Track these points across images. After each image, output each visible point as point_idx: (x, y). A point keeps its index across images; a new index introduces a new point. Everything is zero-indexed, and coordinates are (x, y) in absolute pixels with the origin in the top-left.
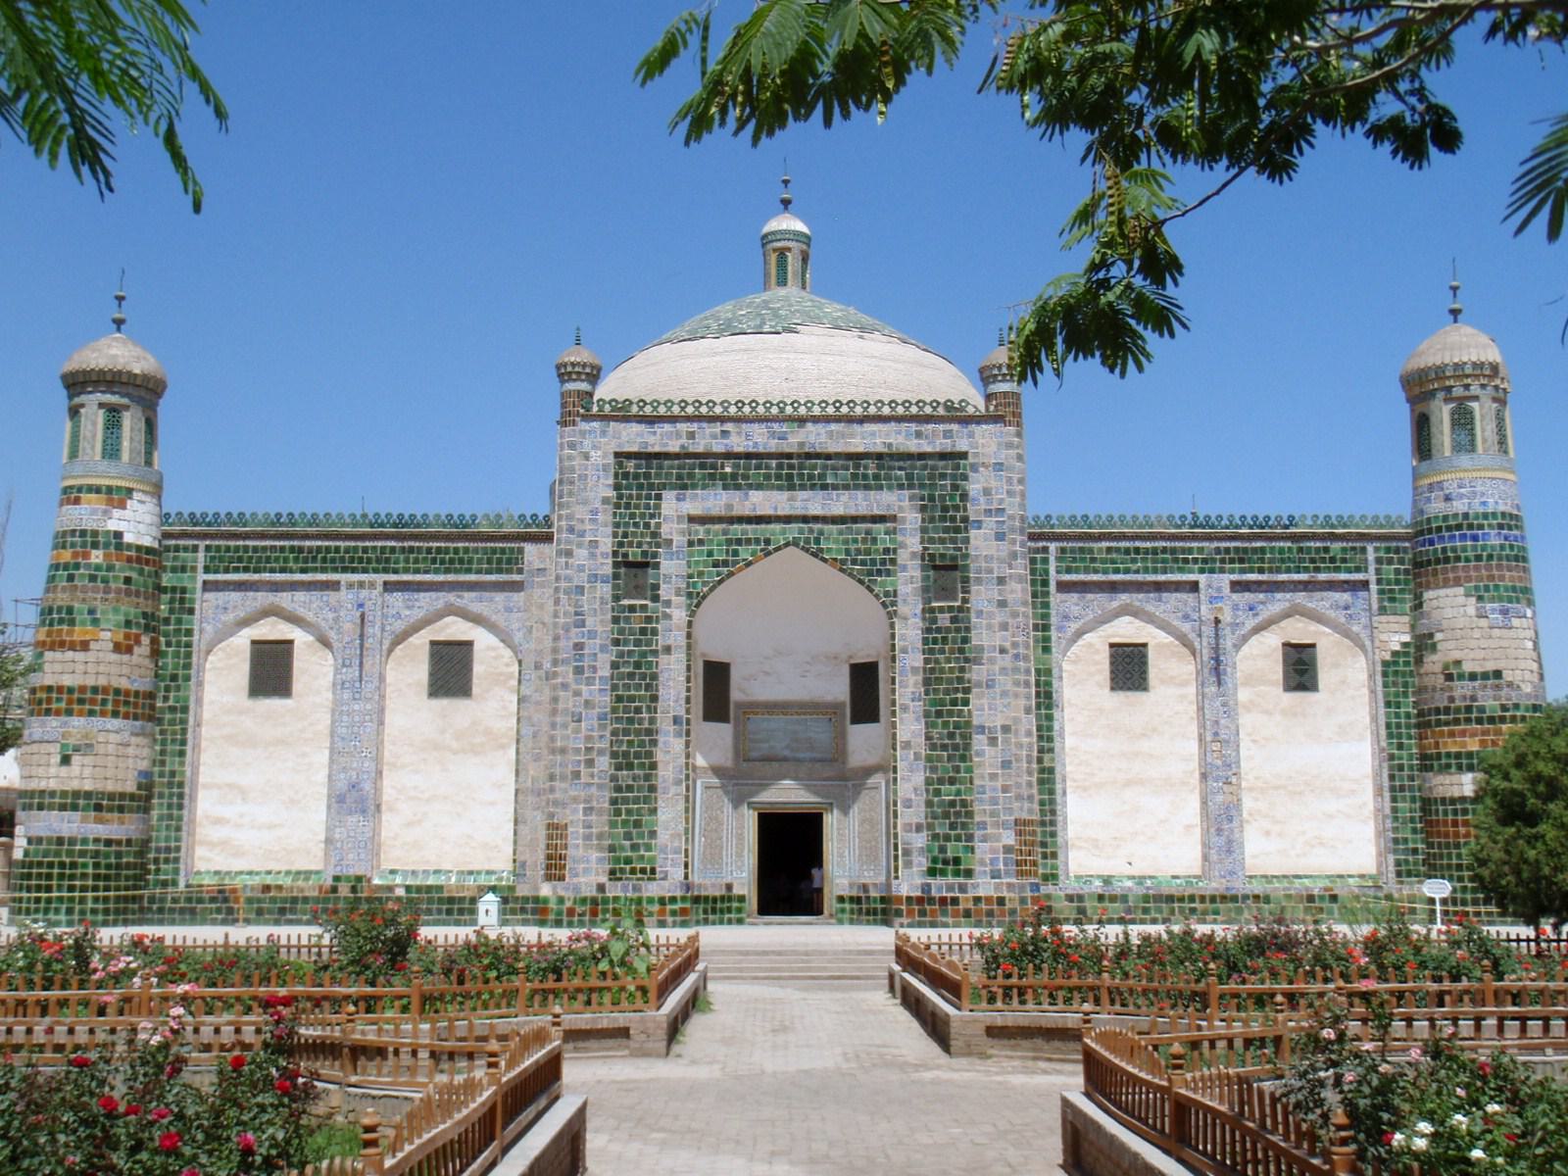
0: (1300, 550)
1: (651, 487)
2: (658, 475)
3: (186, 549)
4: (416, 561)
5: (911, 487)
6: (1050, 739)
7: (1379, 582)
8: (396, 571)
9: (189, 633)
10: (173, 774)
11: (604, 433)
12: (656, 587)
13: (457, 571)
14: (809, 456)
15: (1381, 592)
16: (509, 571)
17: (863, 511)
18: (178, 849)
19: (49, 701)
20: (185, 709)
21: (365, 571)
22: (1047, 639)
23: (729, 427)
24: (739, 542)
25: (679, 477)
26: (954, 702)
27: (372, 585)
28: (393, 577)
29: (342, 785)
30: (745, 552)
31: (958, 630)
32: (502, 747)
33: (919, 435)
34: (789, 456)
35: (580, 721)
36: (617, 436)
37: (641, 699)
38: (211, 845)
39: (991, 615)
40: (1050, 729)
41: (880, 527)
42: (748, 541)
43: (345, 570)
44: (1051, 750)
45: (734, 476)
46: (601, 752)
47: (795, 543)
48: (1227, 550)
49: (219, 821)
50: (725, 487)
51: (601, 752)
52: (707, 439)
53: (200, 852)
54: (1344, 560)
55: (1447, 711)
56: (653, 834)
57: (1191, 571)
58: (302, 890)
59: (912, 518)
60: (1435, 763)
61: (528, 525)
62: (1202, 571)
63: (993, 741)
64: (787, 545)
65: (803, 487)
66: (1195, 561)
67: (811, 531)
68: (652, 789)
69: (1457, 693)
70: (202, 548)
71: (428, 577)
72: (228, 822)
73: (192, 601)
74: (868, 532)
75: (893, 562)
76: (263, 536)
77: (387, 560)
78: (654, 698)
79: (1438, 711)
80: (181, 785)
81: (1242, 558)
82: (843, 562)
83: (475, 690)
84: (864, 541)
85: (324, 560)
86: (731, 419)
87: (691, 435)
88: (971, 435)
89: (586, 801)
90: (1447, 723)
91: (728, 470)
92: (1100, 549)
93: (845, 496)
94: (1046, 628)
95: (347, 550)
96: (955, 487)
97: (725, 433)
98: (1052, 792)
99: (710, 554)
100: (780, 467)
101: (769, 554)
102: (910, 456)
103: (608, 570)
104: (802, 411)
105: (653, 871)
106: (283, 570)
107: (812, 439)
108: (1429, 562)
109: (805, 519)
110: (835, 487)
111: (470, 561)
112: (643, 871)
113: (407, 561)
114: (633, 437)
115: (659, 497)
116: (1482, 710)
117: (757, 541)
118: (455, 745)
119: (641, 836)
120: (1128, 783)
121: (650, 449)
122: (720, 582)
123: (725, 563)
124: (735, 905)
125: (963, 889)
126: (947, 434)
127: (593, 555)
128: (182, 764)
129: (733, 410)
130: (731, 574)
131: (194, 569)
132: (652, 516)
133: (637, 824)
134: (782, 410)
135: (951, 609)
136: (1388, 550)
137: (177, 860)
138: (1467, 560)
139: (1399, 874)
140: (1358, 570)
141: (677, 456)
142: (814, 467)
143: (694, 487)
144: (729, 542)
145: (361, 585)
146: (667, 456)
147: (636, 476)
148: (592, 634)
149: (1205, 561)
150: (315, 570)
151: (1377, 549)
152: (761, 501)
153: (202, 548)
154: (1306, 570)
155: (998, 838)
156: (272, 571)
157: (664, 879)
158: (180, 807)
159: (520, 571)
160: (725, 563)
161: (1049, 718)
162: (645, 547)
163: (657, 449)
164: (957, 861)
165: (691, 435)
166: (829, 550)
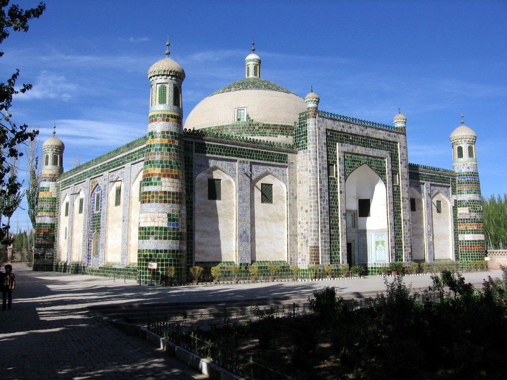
0: (441, 177)
3: (189, 142)
8: (253, 159)
13: (270, 161)
14: (368, 137)
16: (284, 162)
19: (165, 197)
21: (245, 158)
24: (354, 161)
27: (247, 162)
28: (252, 160)
29: (241, 232)
30: (356, 164)
33: (389, 135)
34: (364, 137)
36: (326, 123)
38: (199, 252)
45: (352, 141)
49: (201, 244)
53: (196, 255)
55: (469, 219)
57: (423, 180)
60: (466, 232)
61: (288, 148)
64: (364, 163)
70: (194, 143)
71: (261, 162)
72: (203, 244)
73: (192, 162)
79: (467, 219)
88: (399, 138)
90: (470, 222)
95: (239, 149)
101: (361, 165)
106: (220, 154)
108: (464, 183)
109: (368, 156)
111: (274, 158)
116: (477, 219)
118: (269, 219)
122: (351, 172)
130: (353, 171)
131: (192, 150)
141: (339, 132)
144: (352, 161)
145: (244, 162)
150: (230, 155)
152: (359, 149)
153: (194, 143)
156: (217, 154)
159: (287, 163)
162: (334, 160)
165: (343, 127)
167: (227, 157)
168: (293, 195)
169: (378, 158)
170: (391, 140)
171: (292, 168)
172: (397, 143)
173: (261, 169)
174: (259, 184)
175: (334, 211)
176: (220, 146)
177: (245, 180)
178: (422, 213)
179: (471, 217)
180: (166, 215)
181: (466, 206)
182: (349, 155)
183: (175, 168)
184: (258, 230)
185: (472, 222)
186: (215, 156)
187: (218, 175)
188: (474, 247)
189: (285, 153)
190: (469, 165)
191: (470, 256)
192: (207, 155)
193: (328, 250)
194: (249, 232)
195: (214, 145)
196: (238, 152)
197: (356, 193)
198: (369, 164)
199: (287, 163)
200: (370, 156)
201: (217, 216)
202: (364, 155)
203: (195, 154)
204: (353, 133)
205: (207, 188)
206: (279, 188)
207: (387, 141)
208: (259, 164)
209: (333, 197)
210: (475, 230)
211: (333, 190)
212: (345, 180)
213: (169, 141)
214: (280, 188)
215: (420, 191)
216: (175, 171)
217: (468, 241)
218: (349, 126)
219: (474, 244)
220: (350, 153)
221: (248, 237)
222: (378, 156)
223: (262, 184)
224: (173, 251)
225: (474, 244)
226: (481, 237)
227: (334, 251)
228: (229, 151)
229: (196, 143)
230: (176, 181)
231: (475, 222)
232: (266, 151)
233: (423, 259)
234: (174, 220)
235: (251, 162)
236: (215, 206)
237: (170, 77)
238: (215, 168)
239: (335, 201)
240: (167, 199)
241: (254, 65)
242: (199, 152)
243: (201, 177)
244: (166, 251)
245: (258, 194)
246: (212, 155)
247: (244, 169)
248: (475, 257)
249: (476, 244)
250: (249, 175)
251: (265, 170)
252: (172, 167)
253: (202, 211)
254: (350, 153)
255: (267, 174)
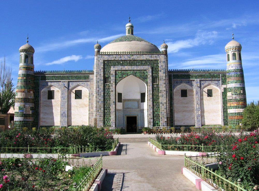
0: (210, 75)
1: (109, 66)
2: (110, 64)
3: (38, 76)
4: (73, 78)
5: (150, 65)
6: (172, 105)
7: (222, 80)
8: (70, 79)
9: (39, 89)
10: (37, 111)
11: (102, 57)
12: (110, 81)
14: (134, 60)
15: (222, 81)
17: (142, 69)
18: (38, 123)
20: (38, 101)
21: (65, 79)
22: (171, 89)
23: (121, 56)
24: (123, 74)
25: (114, 64)
26: (157, 99)
27: (66, 82)
29: (62, 113)
30: (124, 76)
31: (158, 88)
32: (86, 106)
33: (151, 57)
34: (131, 60)
35: (99, 102)
36: (104, 58)
37: (108, 99)
38: (43, 122)
39: (163, 85)
40: (172, 103)
41: (145, 71)
42: (125, 74)
43: (62, 79)
44: (172, 106)
45: (122, 64)
46: (102, 107)
47: (132, 74)
48: (199, 75)
50: (121, 66)
51: (102, 107)
52: (118, 58)
54: (217, 76)
55: (232, 100)
56: (110, 120)
57: (194, 78)
58: (57, 129)
59: (150, 70)
60: (230, 108)
61: (90, 72)
62: (195, 78)
63: (163, 105)
64: (131, 74)
65: (133, 65)
66: (194, 77)
67: (134, 72)
68: (110, 113)
69: (233, 97)
70: (40, 76)
71: (74, 80)
72: (45, 118)
73: (39, 84)
74: (144, 72)
75: (147, 77)
76: (49, 74)
77: (68, 78)
78: (110, 99)
80: (38, 113)
81: (201, 76)
82: (139, 77)
83: (82, 98)
84: (143, 74)
85: (59, 78)
86: (121, 55)
87: (115, 57)
88: (159, 57)
89: (100, 115)
90: (232, 102)
91: (121, 63)
92: (180, 75)
93: (140, 67)
94: (171, 87)
96: (157, 65)
97: (121, 57)
98: (172, 113)
99: (119, 76)
100: (129, 62)
102: (150, 60)
103: (103, 79)
104: (133, 53)
105: (110, 126)
107: (135, 57)
109: (134, 70)
110: (138, 65)
111: (81, 78)
112: (109, 126)
113: (71, 78)
114: (106, 58)
115: (110, 67)
116: (237, 99)
117: (126, 74)
119: (108, 120)
120: (184, 111)
121: (109, 60)
122: (120, 80)
123: (121, 77)
124: (123, 131)
125: (158, 128)
126: (156, 57)
127: (100, 76)
128: (38, 109)
129: (122, 53)
130: (122, 79)
131: (39, 79)
132: (109, 70)
133: (108, 118)
134: (130, 53)
135: (156, 84)
136: (223, 75)
137: (38, 124)
138: (235, 76)
139: (224, 125)
140: (219, 78)
141: (113, 61)
142: (135, 62)
143: (116, 65)
144: (122, 74)
145: (64, 82)
146: (112, 60)
147: (107, 64)
148: (100, 89)
149: (196, 77)
150: (57, 79)
151: (221, 75)
152: (126, 68)
153: (40, 76)
154: (211, 78)
155: (164, 120)
156: (51, 80)
157: (112, 127)
158: (38, 116)
159: (89, 79)
160: (121, 77)
161: (172, 101)
162: (108, 75)
163: (110, 60)
164: (158, 124)
166: (137, 75)
167: (56, 81)
168: (92, 94)
169: (141, 70)
170: (152, 59)
171: (92, 81)
172: (158, 60)
173: (75, 84)
174: (74, 91)
175: (108, 101)
176: (52, 76)
177: (65, 90)
178: (193, 98)
179: (233, 98)
180: (18, 107)
181: (230, 91)
182: (120, 72)
183: (23, 88)
184: (73, 112)
185: (233, 101)
186: (50, 81)
187: (53, 88)
188: (234, 117)
189: (88, 75)
190: (232, 65)
191: (233, 123)
192: (47, 81)
193: (102, 120)
194: (66, 113)
195: (50, 76)
196: (61, 78)
197: (140, 90)
198: (135, 75)
199: (89, 79)
200: (135, 70)
201: (52, 106)
202: (131, 70)
203: (40, 81)
204: (123, 59)
205: (47, 95)
206: (85, 91)
207: (148, 60)
208: (73, 81)
209: (107, 94)
210: (235, 106)
211: (107, 90)
212: (116, 85)
213: (21, 78)
214: (85, 91)
215: (192, 85)
216: (23, 90)
217: (231, 113)
218: (120, 57)
219: (234, 115)
220: (120, 70)
221: (68, 114)
222: (141, 69)
223: (75, 91)
224: (21, 121)
225: (234, 115)
226: (241, 110)
227: (107, 120)
228: (57, 78)
229: (41, 76)
230: (23, 93)
231: (235, 101)
232: (77, 75)
233: (194, 125)
234: (21, 109)
235: (68, 81)
236: (51, 102)
237: (23, 52)
238: (51, 86)
239: (108, 95)
240: (19, 101)
241: (128, 29)
242: (42, 80)
243: (44, 91)
244: (18, 121)
245: (73, 95)
246: (48, 81)
247: (64, 85)
248: (235, 123)
249: (236, 115)
250: (67, 87)
251: (77, 84)
252: (21, 88)
253: (45, 104)
254: (120, 70)
255: (78, 86)
